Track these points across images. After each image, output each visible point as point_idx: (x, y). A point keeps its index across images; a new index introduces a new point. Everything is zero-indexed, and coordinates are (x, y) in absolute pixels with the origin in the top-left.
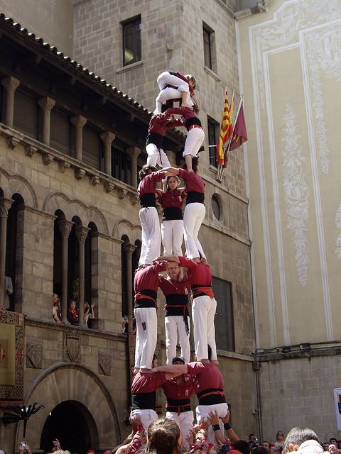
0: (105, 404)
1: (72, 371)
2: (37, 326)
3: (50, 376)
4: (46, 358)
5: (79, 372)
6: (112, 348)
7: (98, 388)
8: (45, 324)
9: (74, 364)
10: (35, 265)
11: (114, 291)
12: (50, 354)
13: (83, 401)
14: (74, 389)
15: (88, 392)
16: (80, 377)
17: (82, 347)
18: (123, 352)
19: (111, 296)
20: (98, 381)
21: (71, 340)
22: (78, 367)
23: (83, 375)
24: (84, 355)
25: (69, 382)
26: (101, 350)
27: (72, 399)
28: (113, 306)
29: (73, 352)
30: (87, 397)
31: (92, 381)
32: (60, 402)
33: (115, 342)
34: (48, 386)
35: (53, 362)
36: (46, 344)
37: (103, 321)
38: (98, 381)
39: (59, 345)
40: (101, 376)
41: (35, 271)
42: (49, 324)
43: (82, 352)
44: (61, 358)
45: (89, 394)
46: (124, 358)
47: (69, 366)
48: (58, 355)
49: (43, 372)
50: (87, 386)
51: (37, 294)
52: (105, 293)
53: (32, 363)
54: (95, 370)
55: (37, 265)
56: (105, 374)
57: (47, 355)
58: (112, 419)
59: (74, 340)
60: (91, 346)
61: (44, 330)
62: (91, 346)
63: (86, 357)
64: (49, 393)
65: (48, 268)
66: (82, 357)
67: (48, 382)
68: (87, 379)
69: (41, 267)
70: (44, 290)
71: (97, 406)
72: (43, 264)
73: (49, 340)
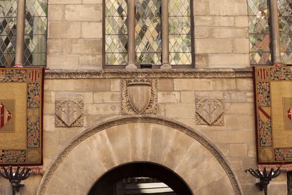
0: (212, 165)
1: (139, 126)
2: (71, 79)
3: (98, 135)
4: (90, 113)
5: (153, 126)
6: (226, 88)
7: (195, 144)
8: (82, 73)
9: (141, 116)
10: (69, 9)
11: (229, 14)
12: (97, 109)
13: (164, 161)
14: (145, 148)
15: (173, 151)
16: (156, 133)
17: (160, 95)
18: (248, 91)
19: (224, 21)
20: (191, 133)
21: (134, 87)
22: (147, 119)
23: (164, 128)
24: (165, 104)
25: (134, 139)
26: (202, 94)
27: (140, 158)
28: (227, 33)
29: (140, 104)
30: (171, 156)
31: (183, 134)
32: (117, 164)
33: (233, 81)
34: (95, 146)
35: (102, 117)
36: (88, 97)
37: (206, 56)
38: (191, 133)
39: (113, 97)
40: (200, 129)
41: (68, 16)
42: (90, 73)
43: (159, 101)
44: (118, 111)
45: (174, 152)
46: (251, 100)
47: (133, 120)
48: (113, 108)
49: (82, 130)
50: (171, 142)
51: (72, 41)
52: (209, 18)
53: (63, 122)
54: (189, 121)
55: (72, 7)
56: (209, 125)
57: (92, 110)
58: (228, 181)
59: (139, 88)
60: (179, 91)
61: (85, 81)
62: (179, 91)
63: (167, 106)
64: (96, 155)
65: (92, 9)
66: (162, 107)
67: (94, 142)
68: (171, 136)
69: (80, 8)
70: (86, 35)
71: (195, 166)
72: (82, 4)
73: (95, 91)
